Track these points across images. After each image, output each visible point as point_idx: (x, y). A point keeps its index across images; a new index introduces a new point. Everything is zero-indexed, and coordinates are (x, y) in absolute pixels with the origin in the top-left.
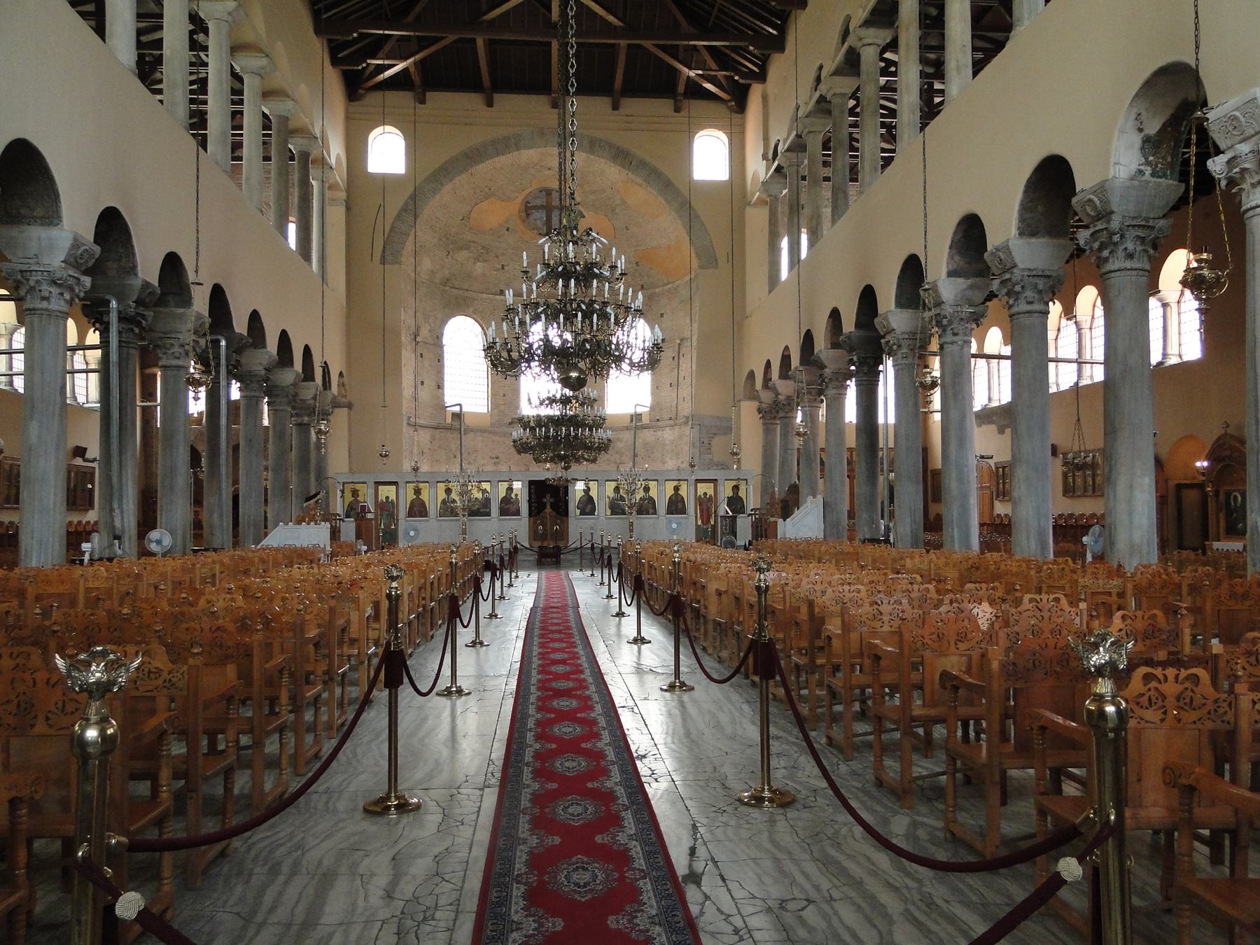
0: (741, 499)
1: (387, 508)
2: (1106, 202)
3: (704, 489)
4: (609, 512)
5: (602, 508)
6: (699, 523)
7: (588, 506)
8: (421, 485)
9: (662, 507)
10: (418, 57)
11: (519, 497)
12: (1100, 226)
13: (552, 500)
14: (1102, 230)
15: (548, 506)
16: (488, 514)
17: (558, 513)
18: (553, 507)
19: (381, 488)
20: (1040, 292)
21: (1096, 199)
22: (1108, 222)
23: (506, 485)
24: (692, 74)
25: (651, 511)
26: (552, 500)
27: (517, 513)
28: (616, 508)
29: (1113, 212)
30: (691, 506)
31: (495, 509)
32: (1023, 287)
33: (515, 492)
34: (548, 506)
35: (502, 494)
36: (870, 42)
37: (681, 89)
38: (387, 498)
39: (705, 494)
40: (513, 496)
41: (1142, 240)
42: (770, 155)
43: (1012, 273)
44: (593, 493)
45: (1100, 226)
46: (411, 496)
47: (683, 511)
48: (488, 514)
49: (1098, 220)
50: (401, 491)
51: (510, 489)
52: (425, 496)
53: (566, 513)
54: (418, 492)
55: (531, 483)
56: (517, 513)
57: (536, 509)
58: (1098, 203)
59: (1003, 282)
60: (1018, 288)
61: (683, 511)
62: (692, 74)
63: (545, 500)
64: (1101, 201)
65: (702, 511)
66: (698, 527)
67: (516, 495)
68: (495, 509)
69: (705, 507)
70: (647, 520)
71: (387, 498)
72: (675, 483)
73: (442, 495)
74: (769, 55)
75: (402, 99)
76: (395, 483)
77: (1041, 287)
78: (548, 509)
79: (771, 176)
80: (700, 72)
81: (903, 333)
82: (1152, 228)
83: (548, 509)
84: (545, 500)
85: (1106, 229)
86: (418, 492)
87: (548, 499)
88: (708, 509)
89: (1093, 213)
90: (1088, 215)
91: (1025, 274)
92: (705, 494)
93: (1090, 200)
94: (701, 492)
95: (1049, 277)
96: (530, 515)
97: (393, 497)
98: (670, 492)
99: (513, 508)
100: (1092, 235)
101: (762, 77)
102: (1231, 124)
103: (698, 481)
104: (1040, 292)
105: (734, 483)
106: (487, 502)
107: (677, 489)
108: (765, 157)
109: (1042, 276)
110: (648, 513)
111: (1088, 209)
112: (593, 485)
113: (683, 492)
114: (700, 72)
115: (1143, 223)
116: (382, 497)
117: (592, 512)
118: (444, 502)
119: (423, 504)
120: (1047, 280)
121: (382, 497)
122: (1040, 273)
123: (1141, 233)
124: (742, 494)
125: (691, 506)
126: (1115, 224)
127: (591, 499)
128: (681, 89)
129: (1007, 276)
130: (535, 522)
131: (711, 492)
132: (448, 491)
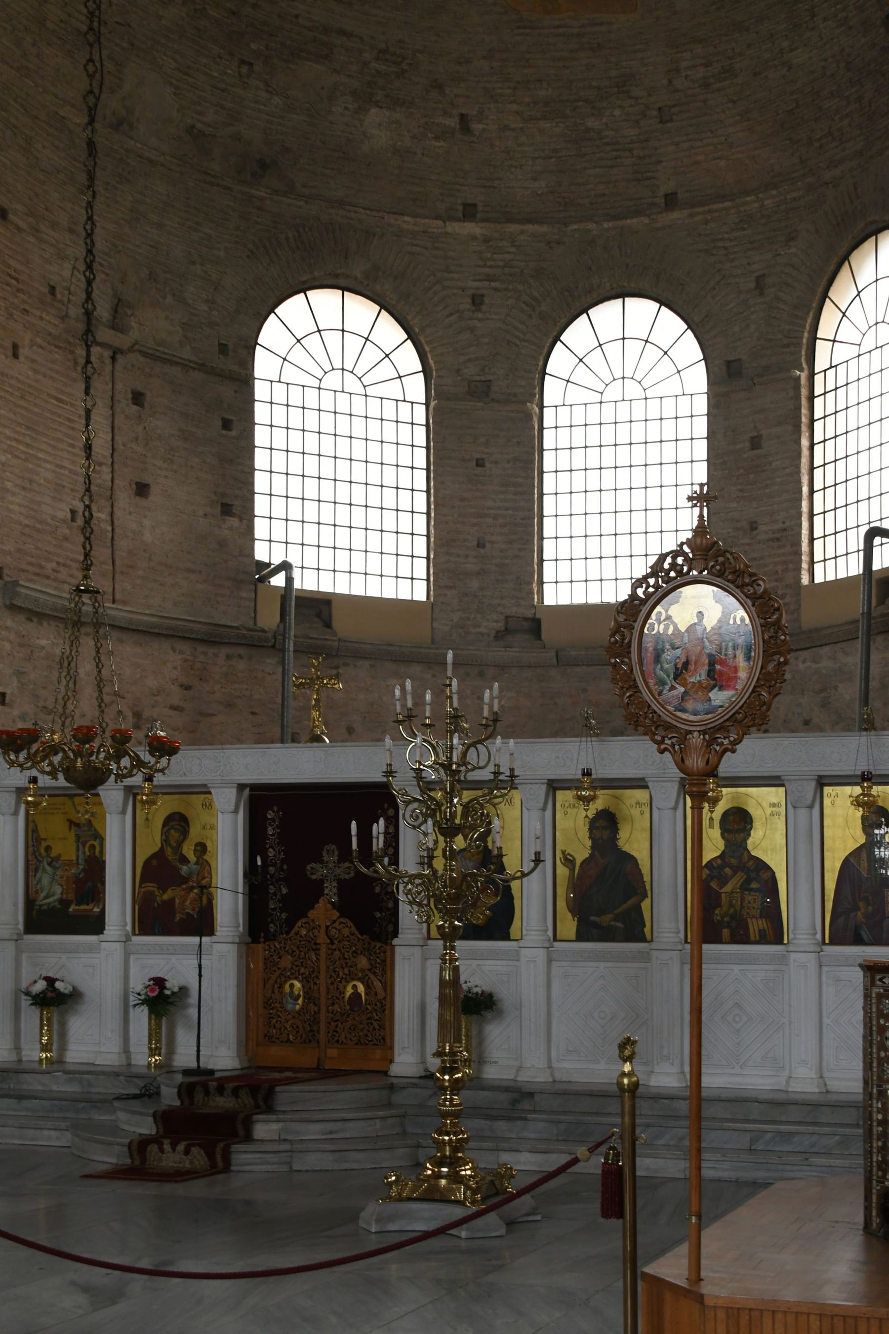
4: (569, 925)
25: (755, 925)
34: (331, 890)
48: (96, 925)
63: (316, 870)
84: (316, 870)
110: (741, 937)
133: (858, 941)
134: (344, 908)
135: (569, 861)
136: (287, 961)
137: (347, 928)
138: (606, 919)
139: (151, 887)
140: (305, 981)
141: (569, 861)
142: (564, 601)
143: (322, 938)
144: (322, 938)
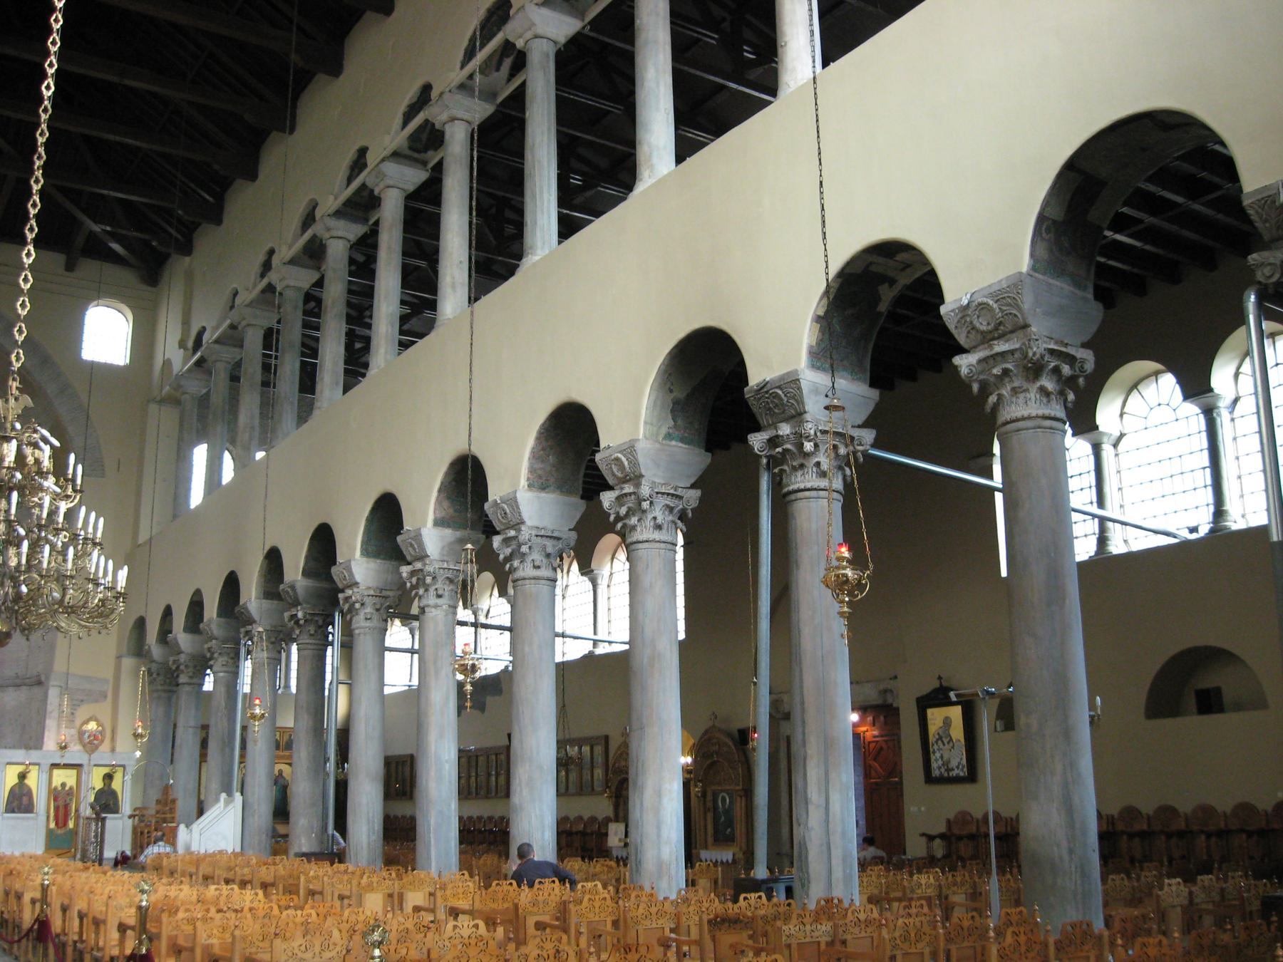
0: (114, 793)
2: (634, 463)
3: (61, 777)
6: (52, 825)
12: (628, 488)
14: (630, 494)
20: (548, 556)
21: (624, 459)
22: (638, 485)
24: (97, 228)
29: (643, 476)
32: (530, 548)
36: (340, 233)
37: (80, 240)
41: (671, 509)
43: (519, 531)
45: (628, 488)
47: (29, 808)
49: (624, 483)
58: (626, 463)
59: (507, 541)
60: (524, 549)
61: (29, 808)
62: (97, 228)
64: (630, 462)
65: (57, 809)
69: (61, 803)
72: (21, 768)
74: (199, 224)
77: (549, 550)
81: (369, 588)
82: (680, 498)
85: (634, 493)
88: (66, 807)
89: (619, 475)
90: (614, 475)
91: (534, 533)
92: (63, 785)
93: (617, 459)
94: (57, 782)
95: (558, 539)
100: (618, 498)
101: (186, 248)
102: (772, 402)
104: (548, 556)
105: (106, 770)
107: (22, 776)
109: (551, 537)
111: (615, 469)
113: (32, 781)
115: (672, 491)
120: (555, 542)
122: (550, 534)
123: (669, 501)
124: (116, 785)
126: (645, 490)
128: (80, 240)
129: (512, 533)
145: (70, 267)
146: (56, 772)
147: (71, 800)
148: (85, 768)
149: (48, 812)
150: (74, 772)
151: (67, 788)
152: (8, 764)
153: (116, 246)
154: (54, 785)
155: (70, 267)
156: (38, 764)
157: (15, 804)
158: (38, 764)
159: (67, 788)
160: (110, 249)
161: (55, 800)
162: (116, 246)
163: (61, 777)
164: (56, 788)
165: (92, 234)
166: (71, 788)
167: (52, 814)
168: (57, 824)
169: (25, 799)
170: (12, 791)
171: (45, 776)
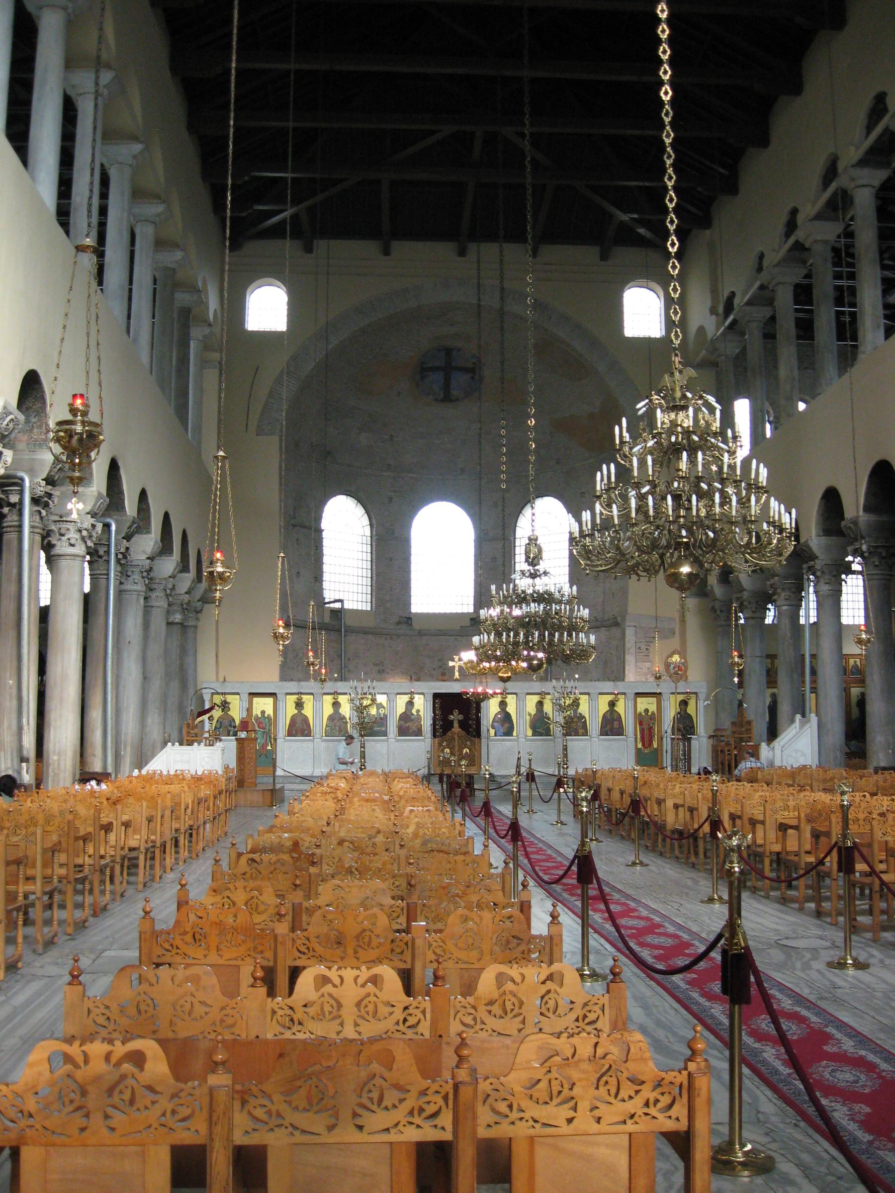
0: (690, 716)
1: (267, 724)
3: (643, 704)
4: (530, 732)
5: (523, 727)
6: (640, 746)
7: (506, 722)
8: (304, 697)
9: (594, 725)
10: (308, 203)
11: (421, 713)
13: (461, 717)
15: (456, 725)
16: (385, 734)
17: (468, 733)
18: (463, 725)
19: (256, 700)
23: (406, 698)
24: (625, 217)
25: (581, 731)
26: (461, 717)
27: (419, 732)
28: (540, 725)
30: (629, 724)
31: (392, 727)
33: (416, 707)
34: (456, 725)
35: (401, 708)
38: (263, 712)
39: (647, 711)
40: (414, 711)
42: (721, 309)
44: (511, 709)
46: (291, 710)
48: (385, 734)
50: (280, 705)
51: (410, 703)
52: (308, 711)
53: (478, 734)
54: (299, 705)
55: (436, 696)
56: (419, 732)
57: (441, 728)
62: (625, 217)
66: (638, 751)
67: (418, 711)
68: (392, 727)
69: (646, 727)
70: (576, 744)
71: (263, 712)
72: (610, 698)
73: (328, 710)
75: (288, 247)
76: (272, 695)
78: (456, 728)
79: (723, 334)
80: (636, 216)
83: (456, 728)
86: (299, 705)
87: (456, 717)
88: (650, 729)
92: (647, 711)
94: (641, 708)
96: (434, 736)
97: (270, 711)
98: (603, 708)
99: (413, 727)
103: (638, 694)
106: (382, 720)
107: (612, 704)
108: (713, 311)
110: (577, 734)
112: (511, 700)
113: (620, 708)
114: (636, 216)
116: (256, 712)
117: (509, 732)
118: (331, 718)
119: (305, 720)
121: (256, 712)
124: (691, 710)
125: (629, 724)
127: (507, 717)
130: (440, 744)
131: (653, 708)
132: (336, 705)
133: (607, 735)
134: (460, 726)
135: (530, 715)
136: (445, 744)
137: (463, 733)
138: (540, 730)
139: (402, 722)
140: (451, 749)
141: (530, 715)
142: (351, 608)
143: (456, 737)
144: (456, 737)
145: (604, 257)
146: (639, 700)
147: (654, 724)
148: (664, 696)
149: (636, 735)
150: (654, 700)
151: (649, 714)
152: (600, 694)
153: (642, 231)
154: (639, 710)
155: (604, 257)
156: (624, 694)
157: (608, 727)
158: (624, 694)
159: (649, 714)
160: (639, 234)
161: (641, 724)
162: (642, 231)
163: (643, 704)
164: (640, 714)
165: (622, 222)
166: (653, 713)
167: (639, 736)
168: (643, 745)
169: (616, 724)
170: (604, 716)
171: (631, 704)
